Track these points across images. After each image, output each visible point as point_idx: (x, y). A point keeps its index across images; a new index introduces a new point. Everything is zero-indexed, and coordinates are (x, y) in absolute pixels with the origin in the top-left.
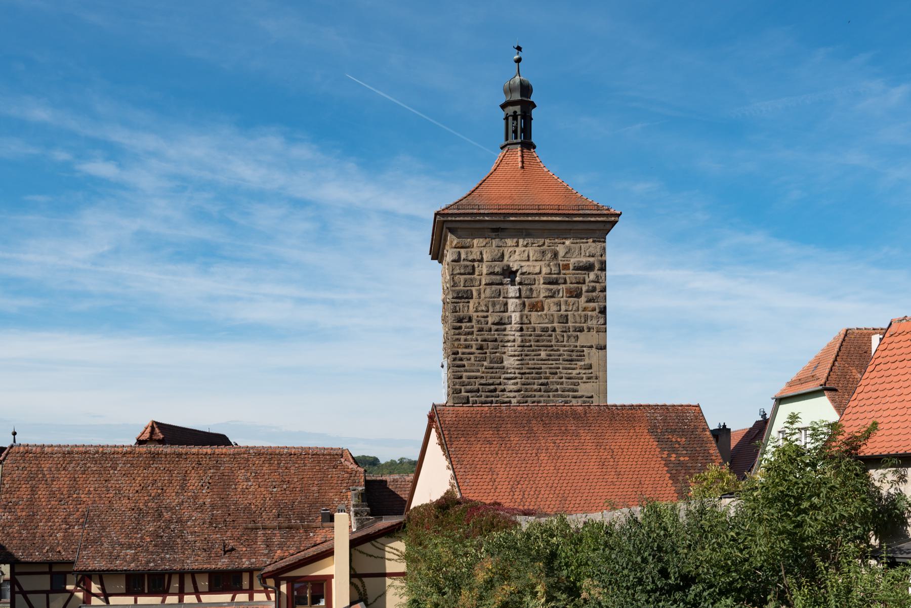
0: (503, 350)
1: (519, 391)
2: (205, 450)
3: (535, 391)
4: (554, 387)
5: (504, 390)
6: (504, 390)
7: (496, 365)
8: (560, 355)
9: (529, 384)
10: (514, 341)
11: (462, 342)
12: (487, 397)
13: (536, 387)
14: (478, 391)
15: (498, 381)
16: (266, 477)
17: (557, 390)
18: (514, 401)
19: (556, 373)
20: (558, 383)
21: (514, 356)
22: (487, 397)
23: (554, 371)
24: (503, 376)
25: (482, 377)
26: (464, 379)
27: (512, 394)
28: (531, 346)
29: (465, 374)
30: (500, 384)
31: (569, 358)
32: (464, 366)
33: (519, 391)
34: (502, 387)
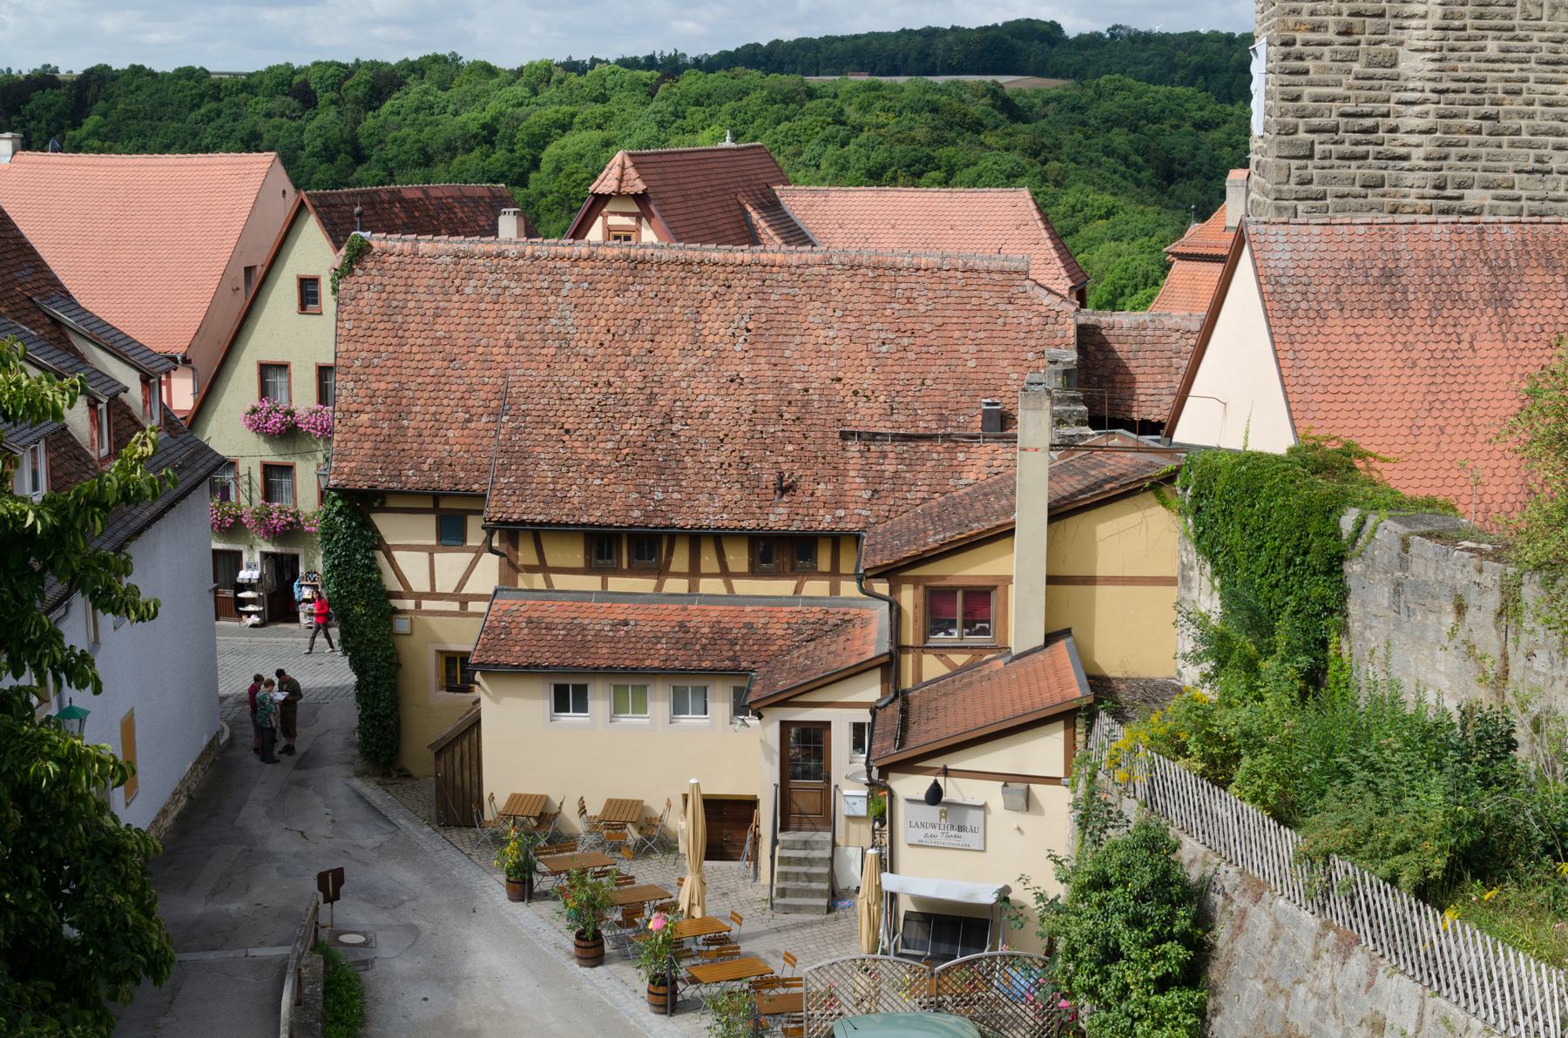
0: (1399, 36)
1: (1430, 131)
2: (739, 256)
3: (1469, 131)
4: (1515, 123)
5: (1394, 130)
6: (1394, 130)
7: (1380, 71)
8: (1530, 51)
9: (1455, 116)
10: (1424, 17)
11: (1305, 17)
12: (1357, 143)
13: (1470, 122)
14: (1335, 130)
15: (1383, 108)
16: (865, 319)
17: (1518, 132)
18: (1417, 154)
19: (1518, 93)
20: (1521, 115)
21: (1425, 50)
22: (1357, 143)
23: (1515, 86)
24: (1396, 96)
25: (1346, 99)
26: (1305, 102)
27: (1415, 139)
28: (1464, 28)
29: (1308, 91)
30: (1387, 115)
31: (1553, 57)
32: (1307, 72)
33: (1430, 131)
34: (1392, 121)
